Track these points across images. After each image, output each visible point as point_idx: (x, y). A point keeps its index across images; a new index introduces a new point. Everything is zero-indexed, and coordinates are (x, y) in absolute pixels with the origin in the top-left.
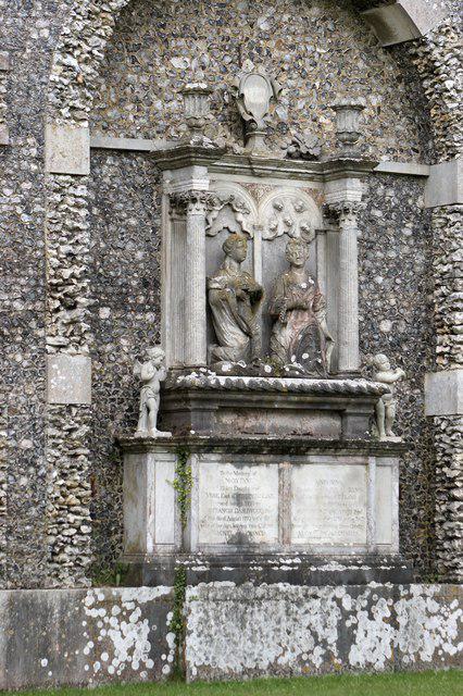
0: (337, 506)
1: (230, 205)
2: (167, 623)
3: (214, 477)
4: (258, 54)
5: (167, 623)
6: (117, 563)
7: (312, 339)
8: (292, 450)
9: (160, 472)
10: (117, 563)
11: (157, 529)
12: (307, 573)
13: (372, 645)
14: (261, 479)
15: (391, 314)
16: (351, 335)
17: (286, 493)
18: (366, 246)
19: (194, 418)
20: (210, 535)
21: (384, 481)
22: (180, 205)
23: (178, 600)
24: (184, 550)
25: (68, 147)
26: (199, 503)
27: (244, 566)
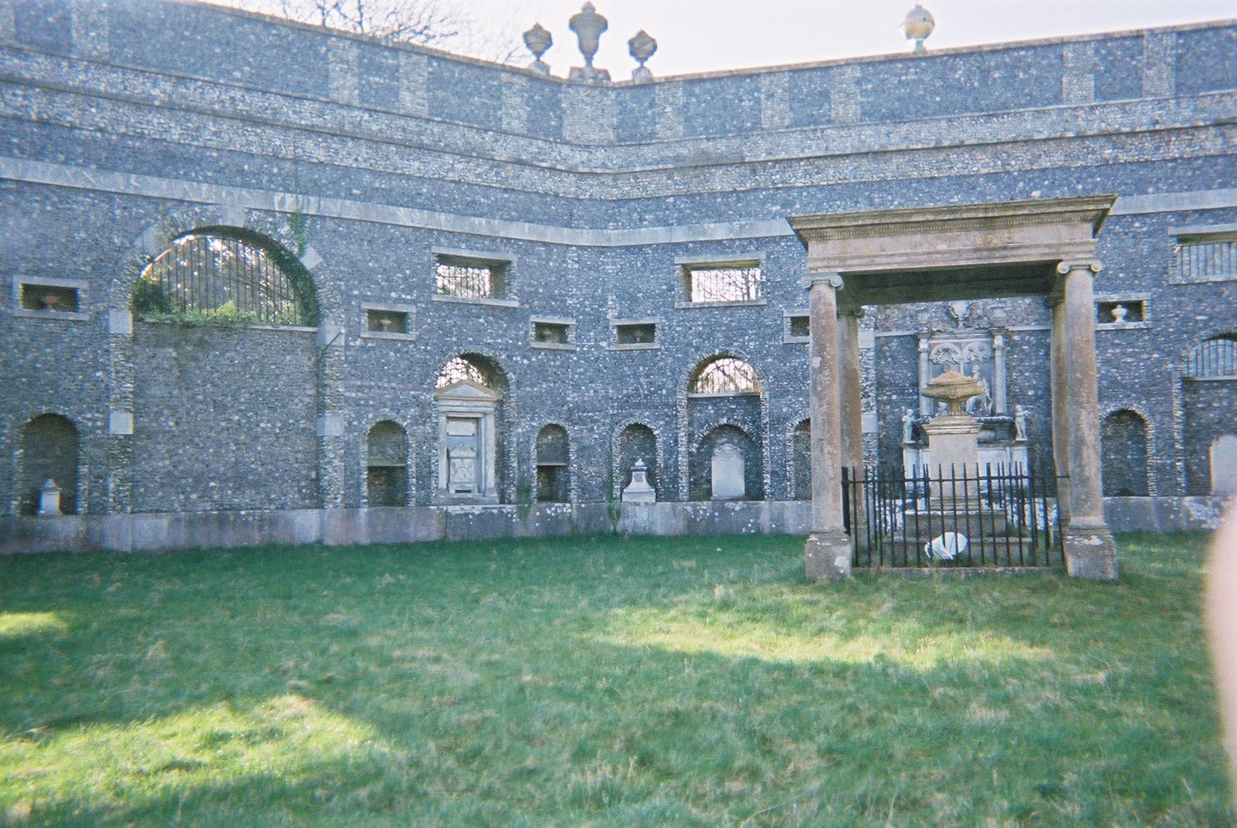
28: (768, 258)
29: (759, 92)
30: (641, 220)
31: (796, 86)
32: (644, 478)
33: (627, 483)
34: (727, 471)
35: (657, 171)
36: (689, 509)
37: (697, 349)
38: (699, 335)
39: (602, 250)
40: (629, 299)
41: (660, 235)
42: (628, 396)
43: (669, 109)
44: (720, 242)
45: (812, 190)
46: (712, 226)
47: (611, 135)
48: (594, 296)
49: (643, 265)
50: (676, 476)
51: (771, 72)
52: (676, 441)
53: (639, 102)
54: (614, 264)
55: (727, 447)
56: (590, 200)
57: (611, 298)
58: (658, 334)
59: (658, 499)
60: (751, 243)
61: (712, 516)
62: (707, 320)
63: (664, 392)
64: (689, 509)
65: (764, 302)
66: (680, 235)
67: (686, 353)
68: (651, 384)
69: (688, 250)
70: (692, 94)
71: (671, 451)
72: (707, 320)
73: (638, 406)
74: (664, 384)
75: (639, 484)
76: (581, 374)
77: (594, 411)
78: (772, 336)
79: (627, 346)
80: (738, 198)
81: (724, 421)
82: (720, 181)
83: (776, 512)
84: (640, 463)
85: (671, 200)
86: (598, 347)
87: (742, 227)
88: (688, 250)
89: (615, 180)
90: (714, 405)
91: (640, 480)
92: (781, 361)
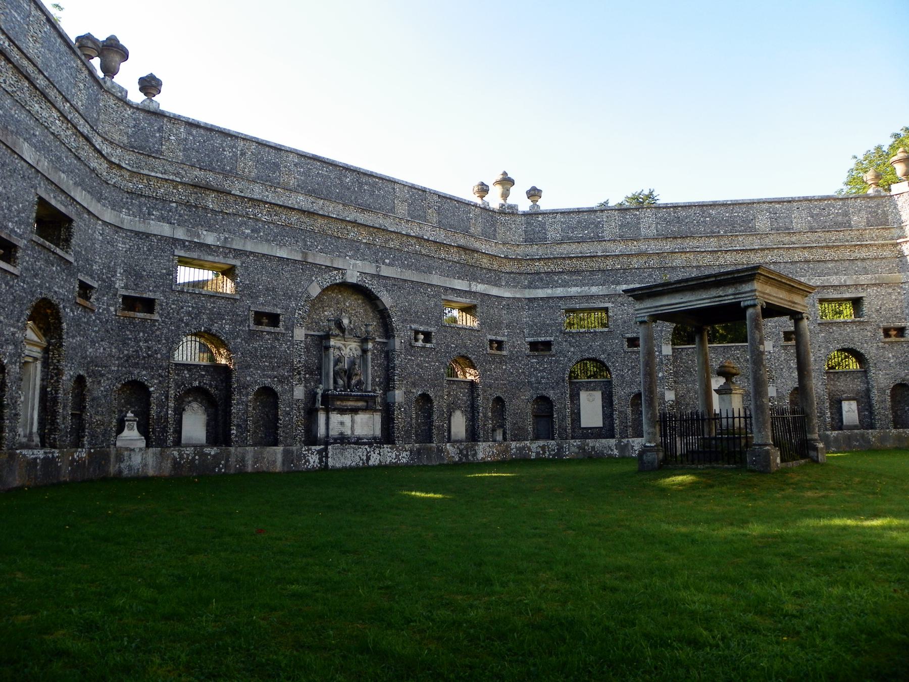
0: (366, 424)
1: (339, 349)
2: (323, 454)
3: (335, 418)
4: (346, 312)
5: (323, 454)
6: (311, 439)
7: (360, 383)
8: (354, 411)
9: (322, 417)
10: (311, 439)
11: (321, 431)
12: (359, 442)
13: (375, 460)
14: (347, 418)
15: (379, 377)
16: (370, 382)
17: (353, 421)
18: (373, 359)
19: (330, 403)
20: (334, 432)
21: (378, 417)
22: (327, 348)
23: (326, 450)
24: (327, 436)
25: (300, 334)
26: (338, 423)
27: (343, 440)
28: (241, 266)
29: (237, 149)
30: (149, 214)
31: (259, 153)
32: (135, 427)
33: (120, 430)
34: (194, 425)
35: (166, 180)
36: (176, 453)
37: (187, 325)
38: (189, 314)
39: (118, 229)
40: (134, 274)
41: (165, 230)
42: (129, 357)
43: (172, 138)
44: (208, 246)
45: (272, 226)
46: (205, 233)
47: (125, 140)
48: (109, 267)
49: (149, 250)
50: (166, 426)
51: (246, 139)
52: (167, 397)
53: (150, 124)
54: (124, 243)
55: (195, 405)
56: (114, 186)
57: (120, 270)
58: (157, 308)
59: (148, 446)
60: (230, 252)
61: (194, 458)
62: (195, 303)
63: (159, 356)
64: (176, 453)
65: (238, 297)
66: (180, 234)
67: (178, 327)
68: (149, 348)
69: (184, 246)
70: (190, 134)
71: (162, 405)
72: (195, 303)
73: (136, 365)
74: (160, 349)
75: (131, 435)
76: (96, 332)
77: (102, 367)
78: (242, 323)
79: (131, 314)
80: (223, 218)
81: (196, 384)
82: (211, 201)
83: (240, 456)
84: (130, 415)
85: (174, 205)
86: (108, 310)
87: (226, 238)
88: (184, 246)
89: (130, 176)
90: (189, 370)
91: (132, 429)
92: (246, 342)
